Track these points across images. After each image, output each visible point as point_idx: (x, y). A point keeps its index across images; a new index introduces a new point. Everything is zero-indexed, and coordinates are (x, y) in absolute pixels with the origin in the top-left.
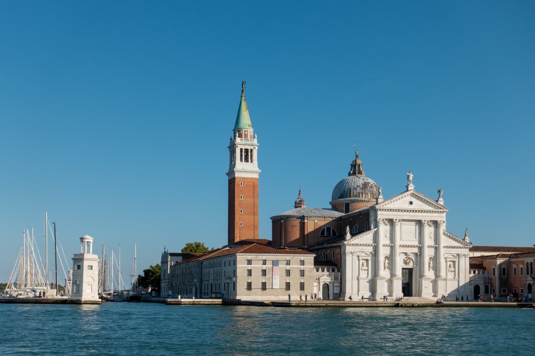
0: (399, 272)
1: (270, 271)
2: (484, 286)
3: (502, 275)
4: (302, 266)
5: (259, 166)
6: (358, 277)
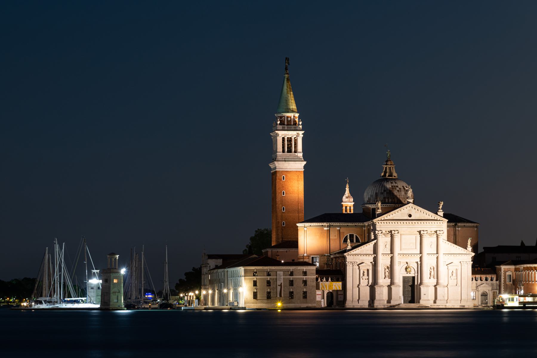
0: (399, 280)
1: (274, 281)
2: (492, 292)
3: (506, 282)
4: (305, 277)
5: (305, 158)
6: (359, 285)
